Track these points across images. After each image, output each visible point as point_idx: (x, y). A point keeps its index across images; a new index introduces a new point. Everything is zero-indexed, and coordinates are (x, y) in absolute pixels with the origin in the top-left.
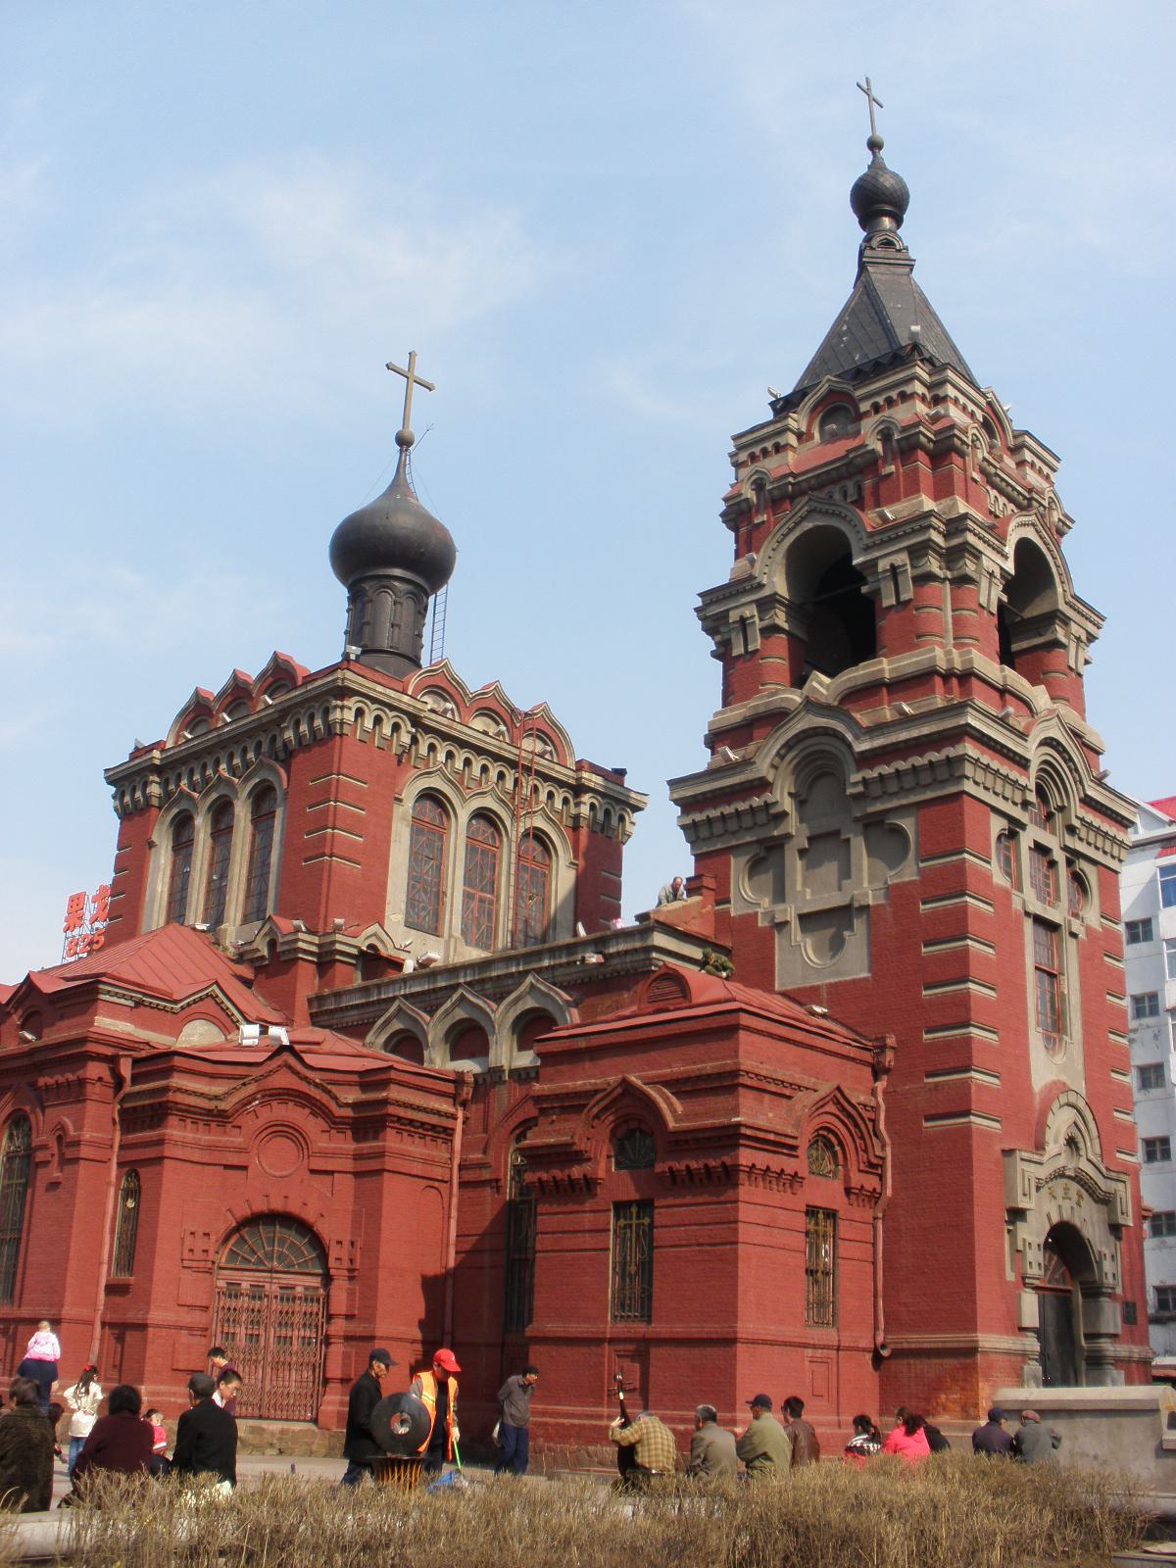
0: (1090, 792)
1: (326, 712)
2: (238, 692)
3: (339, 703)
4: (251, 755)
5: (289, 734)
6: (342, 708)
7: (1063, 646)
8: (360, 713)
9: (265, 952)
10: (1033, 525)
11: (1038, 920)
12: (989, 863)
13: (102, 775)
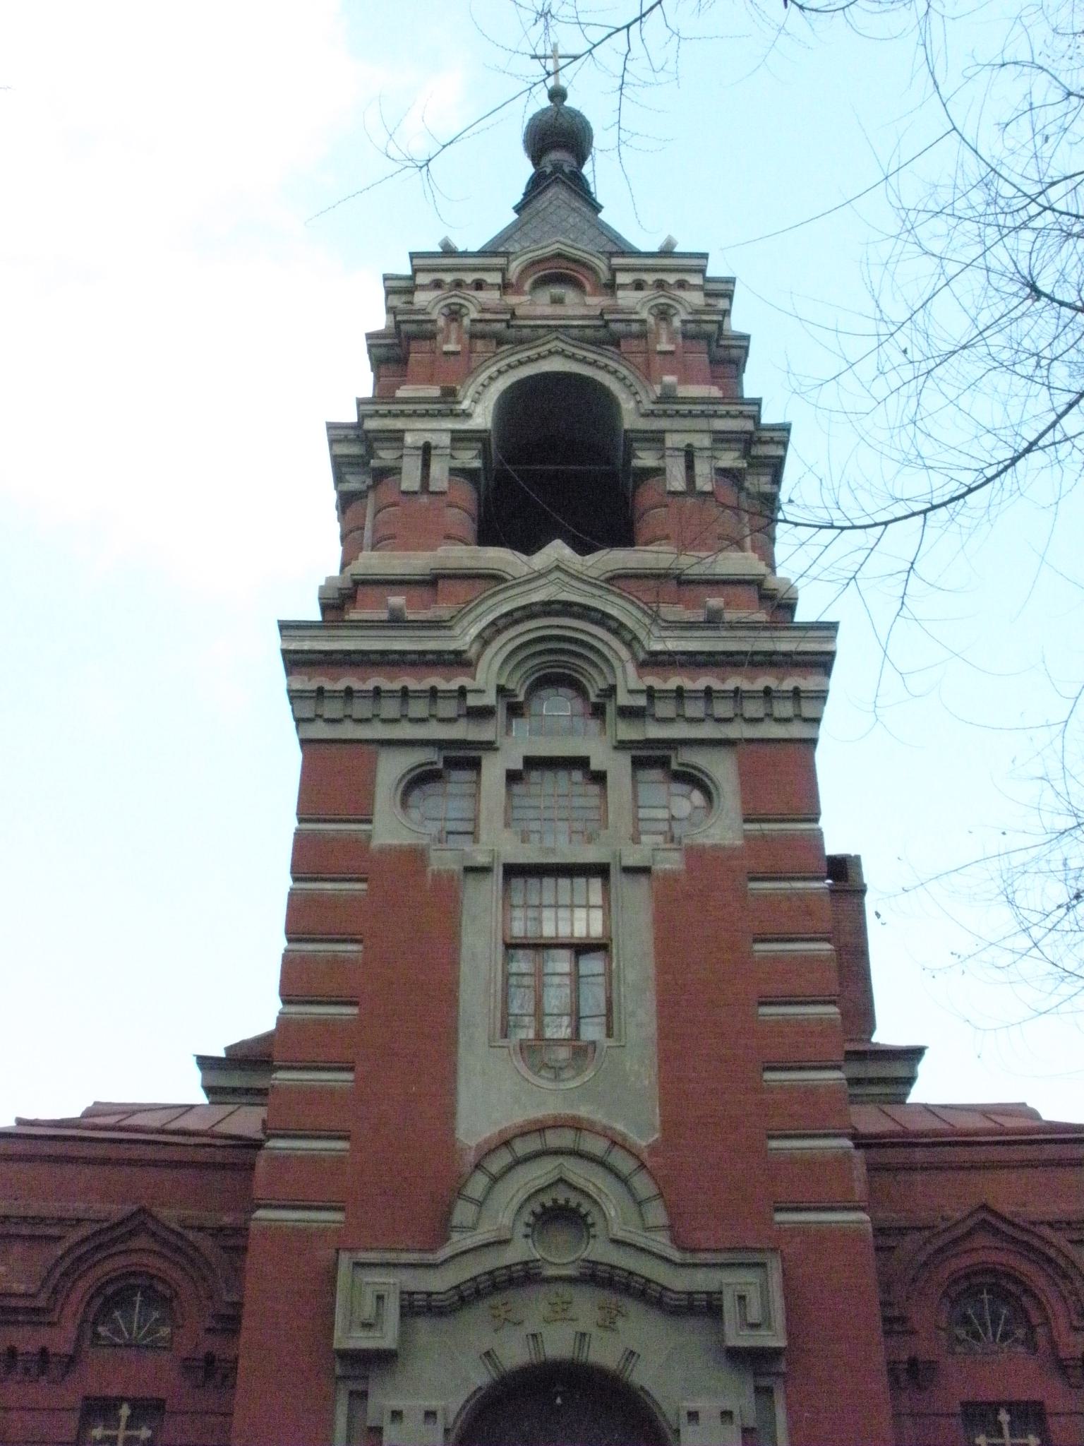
0: (658, 647)
7: (659, 471)
10: (557, 353)
11: (513, 871)
12: (369, 821)
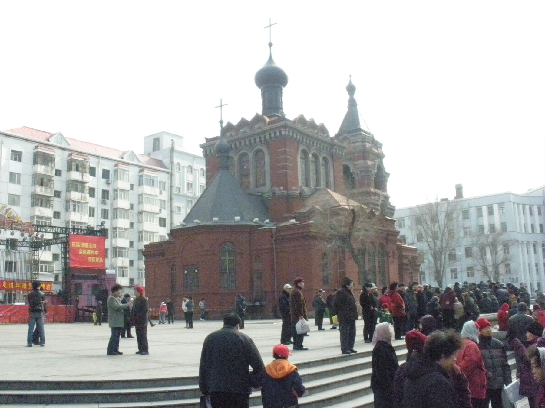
1: (280, 132)
2: (243, 123)
3: (284, 129)
4: (253, 141)
5: (267, 137)
6: (285, 131)
8: (289, 131)
9: (271, 196)
13: (199, 146)
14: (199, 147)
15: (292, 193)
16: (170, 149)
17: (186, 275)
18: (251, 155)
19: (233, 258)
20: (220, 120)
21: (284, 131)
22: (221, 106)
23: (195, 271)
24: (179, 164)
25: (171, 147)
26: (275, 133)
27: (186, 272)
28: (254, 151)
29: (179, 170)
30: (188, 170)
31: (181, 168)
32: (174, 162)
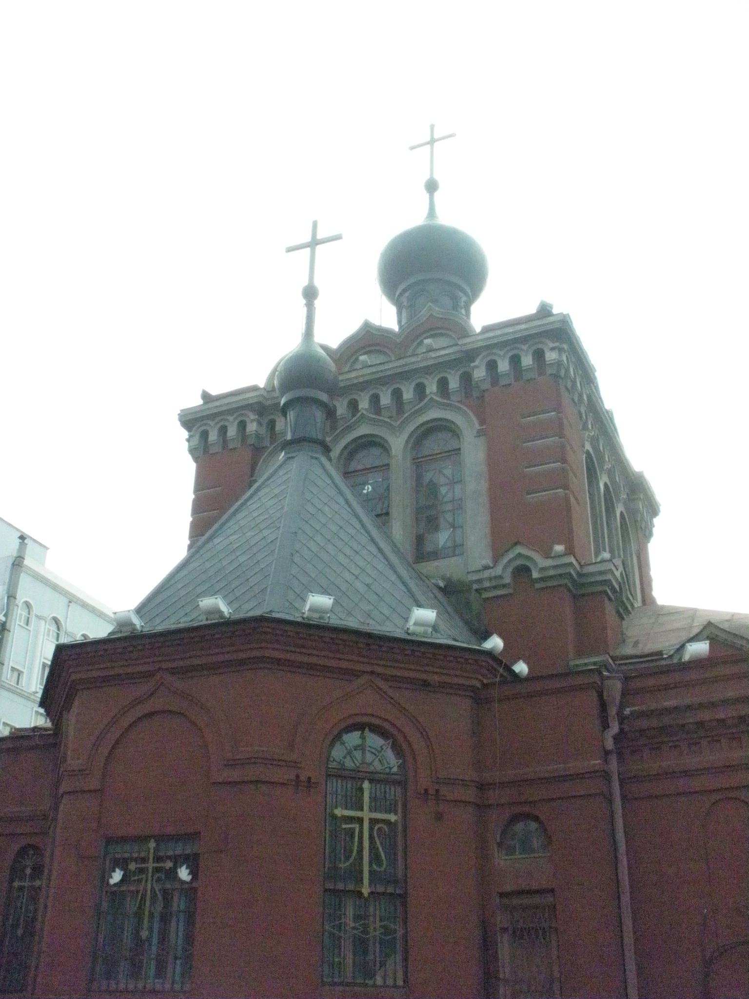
4: (408, 394)
9: (508, 580)
14: (178, 424)
15: (601, 573)
16: (11, 561)
17: (116, 895)
18: (398, 443)
19: (393, 818)
20: (306, 283)
21: (552, 349)
22: (314, 243)
23: (172, 874)
24: (28, 605)
25: (15, 554)
26: (515, 361)
27: (117, 876)
28: (411, 428)
29: (27, 625)
30: (49, 630)
31: (33, 620)
32: (18, 595)
